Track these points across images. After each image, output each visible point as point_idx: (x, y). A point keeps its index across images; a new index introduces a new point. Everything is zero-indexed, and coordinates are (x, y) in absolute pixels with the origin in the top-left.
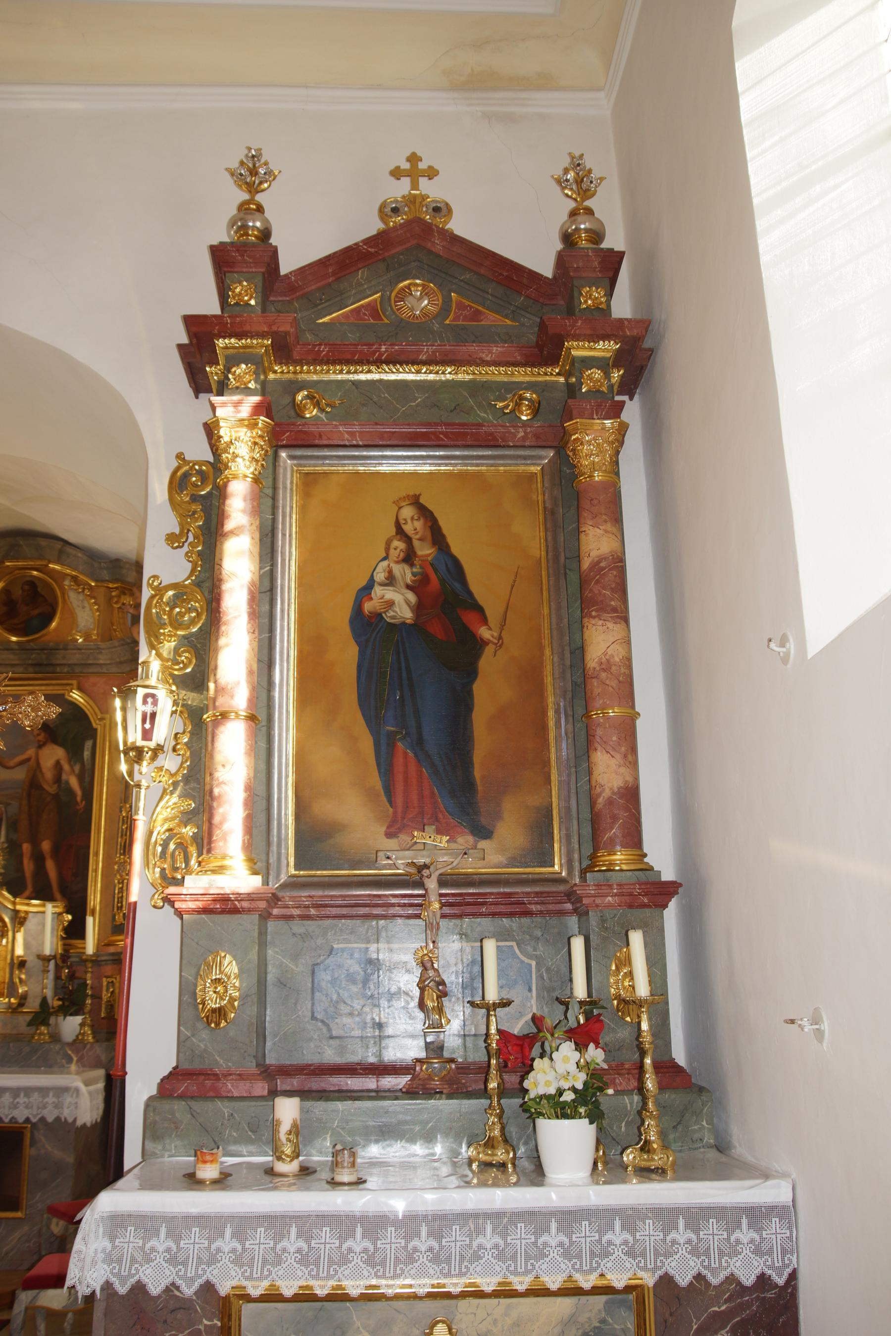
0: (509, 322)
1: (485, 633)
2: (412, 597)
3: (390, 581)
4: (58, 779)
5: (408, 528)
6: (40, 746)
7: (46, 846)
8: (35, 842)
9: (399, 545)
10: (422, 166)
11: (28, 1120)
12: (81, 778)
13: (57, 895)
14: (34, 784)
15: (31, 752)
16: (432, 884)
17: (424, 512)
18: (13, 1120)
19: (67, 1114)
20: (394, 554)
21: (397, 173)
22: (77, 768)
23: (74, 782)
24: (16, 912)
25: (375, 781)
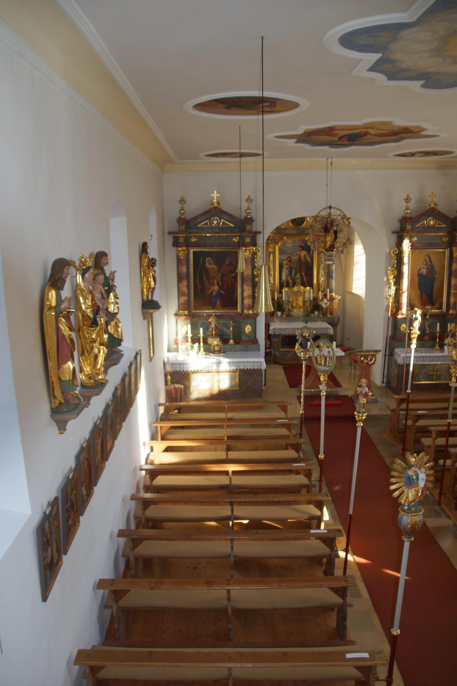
0: (444, 226)
1: (436, 276)
2: (426, 271)
3: (423, 268)
4: (305, 258)
5: (427, 260)
6: (301, 251)
7: (303, 274)
8: (301, 273)
9: (425, 263)
10: (434, 195)
11: (321, 334)
12: (310, 258)
13: (307, 285)
14: (300, 260)
15: (298, 252)
16: (428, 314)
17: (429, 257)
18: (319, 334)
19: (329, 332)
20: (424, 264)
21: (429, 196)
22: (309, 256)
23: (309, 259)
24: (304, 291)
25: (420, 298)
